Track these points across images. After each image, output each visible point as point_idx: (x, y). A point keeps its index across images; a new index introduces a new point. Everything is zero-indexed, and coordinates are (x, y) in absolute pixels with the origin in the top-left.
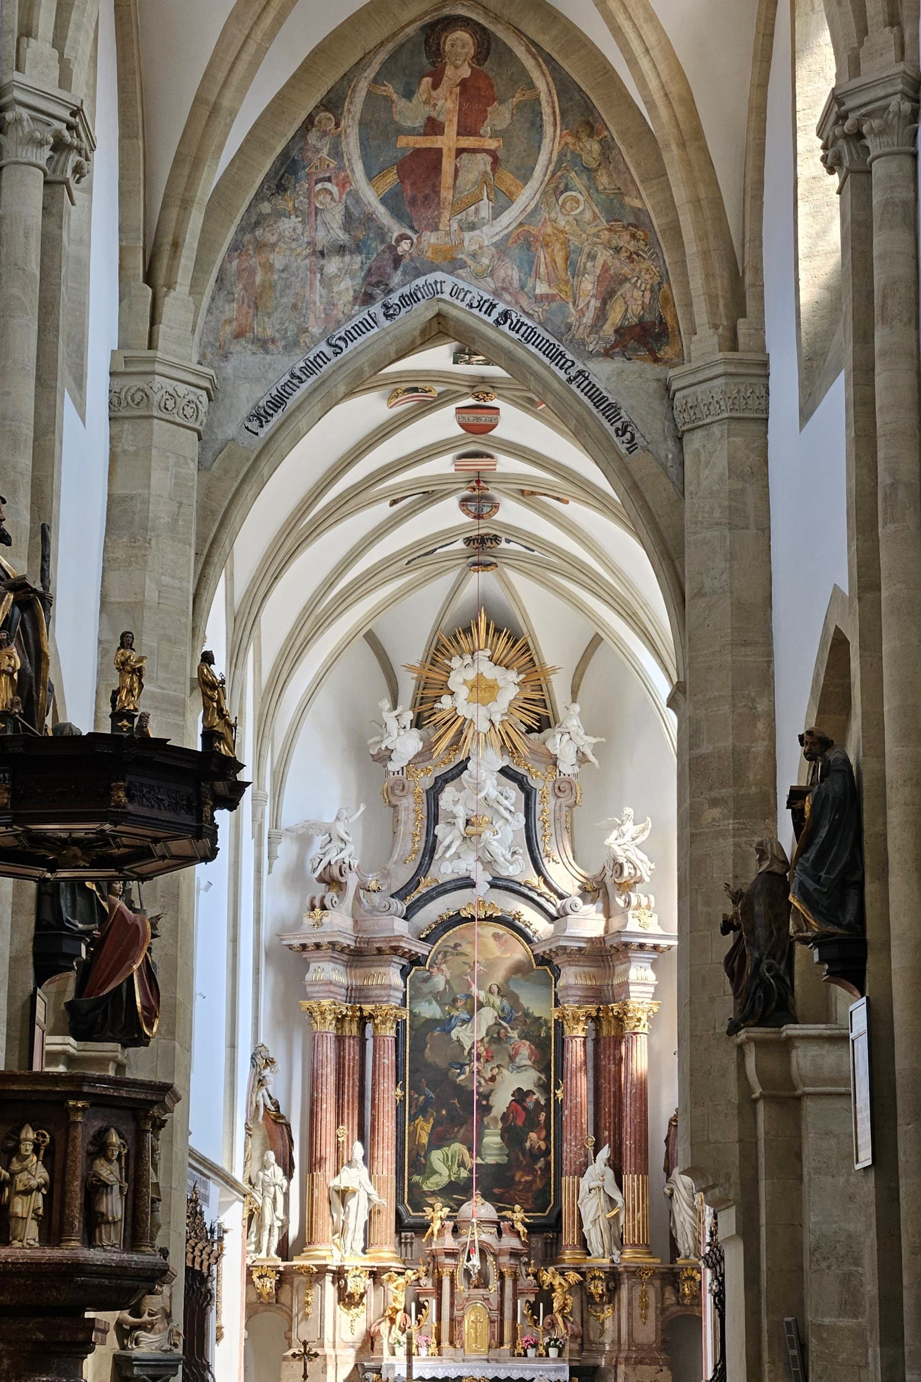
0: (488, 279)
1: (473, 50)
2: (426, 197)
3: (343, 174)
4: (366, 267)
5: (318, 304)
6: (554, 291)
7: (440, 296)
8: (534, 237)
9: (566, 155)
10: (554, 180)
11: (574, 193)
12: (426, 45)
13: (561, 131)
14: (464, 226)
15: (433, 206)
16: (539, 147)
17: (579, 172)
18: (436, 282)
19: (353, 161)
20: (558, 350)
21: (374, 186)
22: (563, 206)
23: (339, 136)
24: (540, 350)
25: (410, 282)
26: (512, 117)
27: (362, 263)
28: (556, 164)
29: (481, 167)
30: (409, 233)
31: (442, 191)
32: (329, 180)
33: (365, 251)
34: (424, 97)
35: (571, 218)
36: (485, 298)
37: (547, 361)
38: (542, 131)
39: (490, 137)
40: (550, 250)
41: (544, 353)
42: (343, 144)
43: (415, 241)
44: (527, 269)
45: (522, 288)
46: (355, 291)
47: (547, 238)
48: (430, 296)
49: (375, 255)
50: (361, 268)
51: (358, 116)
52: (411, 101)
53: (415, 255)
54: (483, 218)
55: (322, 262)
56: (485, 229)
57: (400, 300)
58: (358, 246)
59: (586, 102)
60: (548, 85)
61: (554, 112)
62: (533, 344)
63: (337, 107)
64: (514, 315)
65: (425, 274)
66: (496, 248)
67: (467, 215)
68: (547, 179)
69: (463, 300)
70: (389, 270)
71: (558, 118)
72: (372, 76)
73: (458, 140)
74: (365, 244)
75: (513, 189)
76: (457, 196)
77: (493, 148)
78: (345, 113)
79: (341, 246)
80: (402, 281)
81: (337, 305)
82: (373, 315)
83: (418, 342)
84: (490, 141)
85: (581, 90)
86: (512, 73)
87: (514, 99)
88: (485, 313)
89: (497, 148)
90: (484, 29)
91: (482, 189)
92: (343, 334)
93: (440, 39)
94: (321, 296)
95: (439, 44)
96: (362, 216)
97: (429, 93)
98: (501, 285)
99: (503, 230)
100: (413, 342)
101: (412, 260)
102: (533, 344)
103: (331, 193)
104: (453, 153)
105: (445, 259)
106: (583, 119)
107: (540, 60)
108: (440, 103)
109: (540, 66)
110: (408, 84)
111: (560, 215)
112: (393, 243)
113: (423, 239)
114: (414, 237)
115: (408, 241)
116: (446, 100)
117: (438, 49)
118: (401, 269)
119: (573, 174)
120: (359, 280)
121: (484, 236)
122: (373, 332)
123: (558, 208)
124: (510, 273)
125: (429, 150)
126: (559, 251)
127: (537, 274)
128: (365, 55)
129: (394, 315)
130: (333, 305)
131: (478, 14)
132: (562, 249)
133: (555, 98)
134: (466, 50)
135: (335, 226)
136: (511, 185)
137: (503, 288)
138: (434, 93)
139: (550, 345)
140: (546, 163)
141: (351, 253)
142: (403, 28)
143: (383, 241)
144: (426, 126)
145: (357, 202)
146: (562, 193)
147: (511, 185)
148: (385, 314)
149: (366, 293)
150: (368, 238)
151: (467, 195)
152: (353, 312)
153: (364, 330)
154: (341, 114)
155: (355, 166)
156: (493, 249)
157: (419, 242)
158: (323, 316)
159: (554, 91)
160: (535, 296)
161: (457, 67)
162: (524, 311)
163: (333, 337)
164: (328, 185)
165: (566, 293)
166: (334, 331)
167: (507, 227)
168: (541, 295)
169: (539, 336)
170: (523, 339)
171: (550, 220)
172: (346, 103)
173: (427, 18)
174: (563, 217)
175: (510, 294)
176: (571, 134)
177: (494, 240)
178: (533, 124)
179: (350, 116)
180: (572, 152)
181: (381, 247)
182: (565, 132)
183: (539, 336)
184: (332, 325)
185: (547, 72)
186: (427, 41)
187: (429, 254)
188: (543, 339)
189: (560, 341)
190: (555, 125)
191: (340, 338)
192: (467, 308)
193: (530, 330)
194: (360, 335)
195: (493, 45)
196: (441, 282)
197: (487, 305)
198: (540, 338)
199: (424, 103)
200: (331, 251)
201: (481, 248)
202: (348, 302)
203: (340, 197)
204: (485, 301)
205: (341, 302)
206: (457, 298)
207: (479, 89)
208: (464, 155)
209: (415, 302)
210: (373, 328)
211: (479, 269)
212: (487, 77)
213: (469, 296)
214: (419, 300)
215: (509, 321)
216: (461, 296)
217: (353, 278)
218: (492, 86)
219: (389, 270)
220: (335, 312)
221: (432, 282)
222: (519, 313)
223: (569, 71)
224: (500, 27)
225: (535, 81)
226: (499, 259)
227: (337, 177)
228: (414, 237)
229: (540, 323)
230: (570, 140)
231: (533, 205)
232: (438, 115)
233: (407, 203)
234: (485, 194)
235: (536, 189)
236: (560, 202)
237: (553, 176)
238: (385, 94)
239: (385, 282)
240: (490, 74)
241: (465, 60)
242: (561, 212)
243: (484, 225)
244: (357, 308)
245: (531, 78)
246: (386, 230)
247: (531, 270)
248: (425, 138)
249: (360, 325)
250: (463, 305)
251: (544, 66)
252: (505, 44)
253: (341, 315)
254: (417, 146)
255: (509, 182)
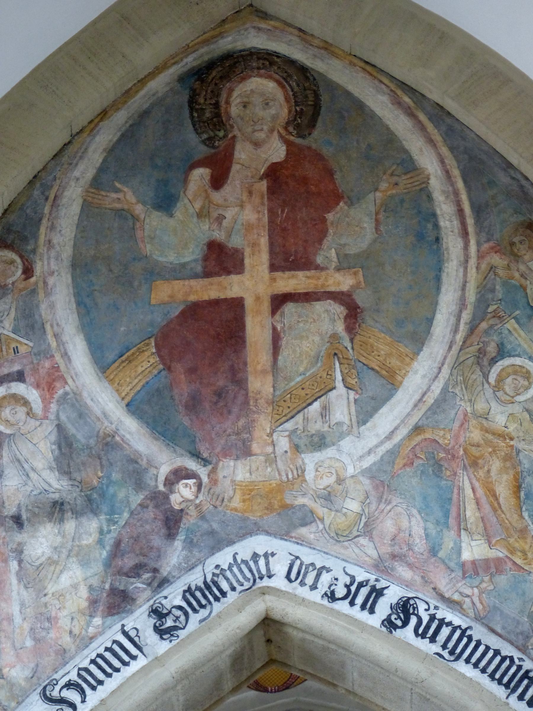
0: (363, 541)
1: (286, 111)
2: (219, 394)
3: (47, 364)
4: (110, 540)
5: (18, 619)
6: (499, 553)
7: (266, 582)
8: (447, 451)
9: (493, 290)
10: (475, 339)
11: (518, 361)
12: (192, 109)
13: (479, 244)
14: (302, 443)
15: (235, 410)
16: (438, 279)
17: (524, 320)
18: (255, 556)
19: (65, 338)
20: (520, 667)
21: (111, 381)
22: (498, 386)
23: (34, 292)
24: (483, 671)
25: (201, 562)
26: (377, 229)
27: (101, 532)
28: (476, 307)
29: (326, 327)
30: (192, 465)
31: (251, 379)
32: (20, 377)
33: (105, 508)
34: (198, 205)
35: (516, 409)
36: (359, 579)
37: (501, 692)
38: (439, 249)
39: (338, 269)
40: (481, 473)
41: (492, 676)
42: (43, 307)
43: (205, 479)
44: (439, 514)
45: (433, 551)
46: (91, 588)
47: (474, 451)
48: (247, 585)
49: (126, 515)
50: (100, 542)
51: (67, 252)
52: (171, 216)
53: (207, 507)
54: (339, 424)
55: (19, 537)
56: (346, 443)
57: (184, 598)
58: (89, 500)
59: (522, 187)
60: (442, 161)
61: (460, 212)
62: (467, 661)
63: (25, 239)
64: (422, 607)
65: (231, 543)
66: (372, 478)
67: (306, 420)
68: (459, 337)
69: (314, 587)
70: (157, 541)
71: (470, 221)
72: (90, 174)
73: (274, 280)
74: (103, 495)
75: (394, 362)
76: (282, 385)
77: (345, 288)
78: (42, 249)
79: (55, 503)
80: (187, 559)
81: (56, 618)
82: (132, 634)
83: (228, 685)
84: (338, 277)
85: (510, 165)
86: (370, 147)
87: (378, 194)
88: (363, 607)
89: (357, 286)
90: (303, 70)
91: (332, 368)
92: (73, 676)
93: (218, 95)
94: (22, 605)
95: (217, 105)
96: (92, 442)
97: (207, 197)
98: (389, 550)
99: (382, 443)
100: (218, 684)
101: (202, 517)
102: (467, 661)
103: (26, 403)
104: (266, 306)
105: (270, 508)
106: (521, 218)
107: (422, 117)
108: (229, 214)
109: (423, 128)
110: (164, 183)
111: (493, 404)
112: (161, 488)
113: (221, 474)
114: (203, 472)
115: (191, 482)
116: (242, 206)
117: (218, 115)
118: (181, 537)
119: (511, 324)
120: (97, 567)
121: (346, 459)
122: (135, 666)
123: (489, 392)
124: (405, 524)
125: (216, 303)
126: (500, 472)
127: (460, 519)
128: (73, 136)
129: (176, 628)
130: (49, 619)
131: (289, 43)
132: (503, 470)
133: (460, 184)
134: (273, 111)
135: (39, 464)
136: (390, 355)
137: (394, 556)
138: (217, 196)
139: (504, 659)
140: (454, 308)
141: (77, 514)
142: (142, 82)
143: (139, 485)
144: (206, 259)
145: (81, 415)
146: (493, 361)
147: (390, 355)
148: (157, 629)
149: (113, 591)
150: (110, 482)
151: (303, 382)
152: (91, 630)
153: (116, 663)
154: (34, 251)
155: (70, 347)
156: (366, 482)
157: (214, 482)
158: (29, 643)
159: (456, 172)
160: (463, 565)
161: (257, 144)
162: (442, 597)
163: (53, 683)
164: (18, 388)
165: (524, 553)
166: (56, 671)
167: (389, 437)
168: (473, 562)
169: (479, 643)
170: (445, 654)
171: (478, 416)
172: (43, 230)
173: (190, 59)
174: (500, 408)
175: (410, 566)
176: (496, 249)
177: (367, 463)
178: (420, 237)
179: (53, 254)
180: (505, 284)
181: (137, 499)
182: (486, 246)
183: (479, 643)
184: (48, 660)
185: (437, 138)
186: (192, 102)
187: (236, 503)
188: (488, 648)
189: (523, 649)
190: (465, 234)
191: (69, 685)
192: (325, 602)
193: (458, 633)
194: (109, 675)
195: (325, 98)
196: (266, 555)
197: (364, 592)
198: (482, 649)
199: (199, 215)
200: (35, 515)
201: (340, 481)
202: (81, 612)
203: (46, 409)
204: (361, 585)
205: (65, 612)
206: (302, 584)
207: (305, 181)
208: (289, 308)
209: (217, 599)
210: (134, 658)
211: (341, 521)
212: (319, 157)
213: (325, 578)
214: (224, 594)
215: (413, 620)
216: (310, 579)
217: (85, 563)
218: (330, 173)
219: (157, 541)
220: (52, 634)
221: (247, 556)
222: (433, 603)
223: (482, 130)
224: (336, 63)
225: (416, 157)
226: (380, 499)
227: (35, 370)
228: (203, 472)
229: (478, 619)
230: (496, 260)
231: (437, 389)
232: (229, 235)
233: (181, 408)
234: (339, 377)
235: (440, 358)
236: (492, 379)
237: (472, 330)
238: (118, 206)
239: (153, 564)
240: (327, 151)
241: (272, 131)
242: (498, 399)
243: (342, 436)
244: (97, 621)
245: (406, 152)
246: (144, 463)
247: (447, 515)
248: (207, 281)
249: (108, 655)
250: (316, 596)
251: (430, 127)
252: (348, 94)
253: (67, 640)
254: (193, 298)
255: (384, 349)
